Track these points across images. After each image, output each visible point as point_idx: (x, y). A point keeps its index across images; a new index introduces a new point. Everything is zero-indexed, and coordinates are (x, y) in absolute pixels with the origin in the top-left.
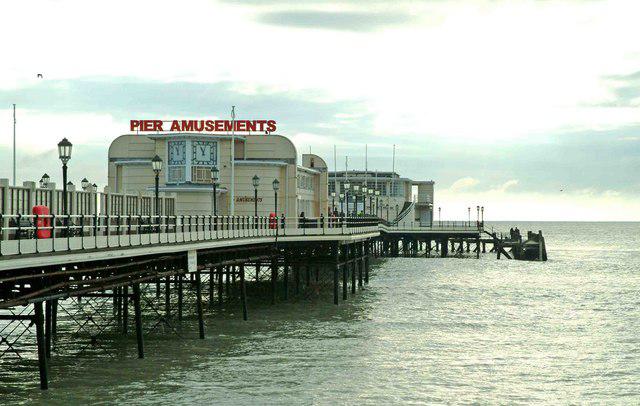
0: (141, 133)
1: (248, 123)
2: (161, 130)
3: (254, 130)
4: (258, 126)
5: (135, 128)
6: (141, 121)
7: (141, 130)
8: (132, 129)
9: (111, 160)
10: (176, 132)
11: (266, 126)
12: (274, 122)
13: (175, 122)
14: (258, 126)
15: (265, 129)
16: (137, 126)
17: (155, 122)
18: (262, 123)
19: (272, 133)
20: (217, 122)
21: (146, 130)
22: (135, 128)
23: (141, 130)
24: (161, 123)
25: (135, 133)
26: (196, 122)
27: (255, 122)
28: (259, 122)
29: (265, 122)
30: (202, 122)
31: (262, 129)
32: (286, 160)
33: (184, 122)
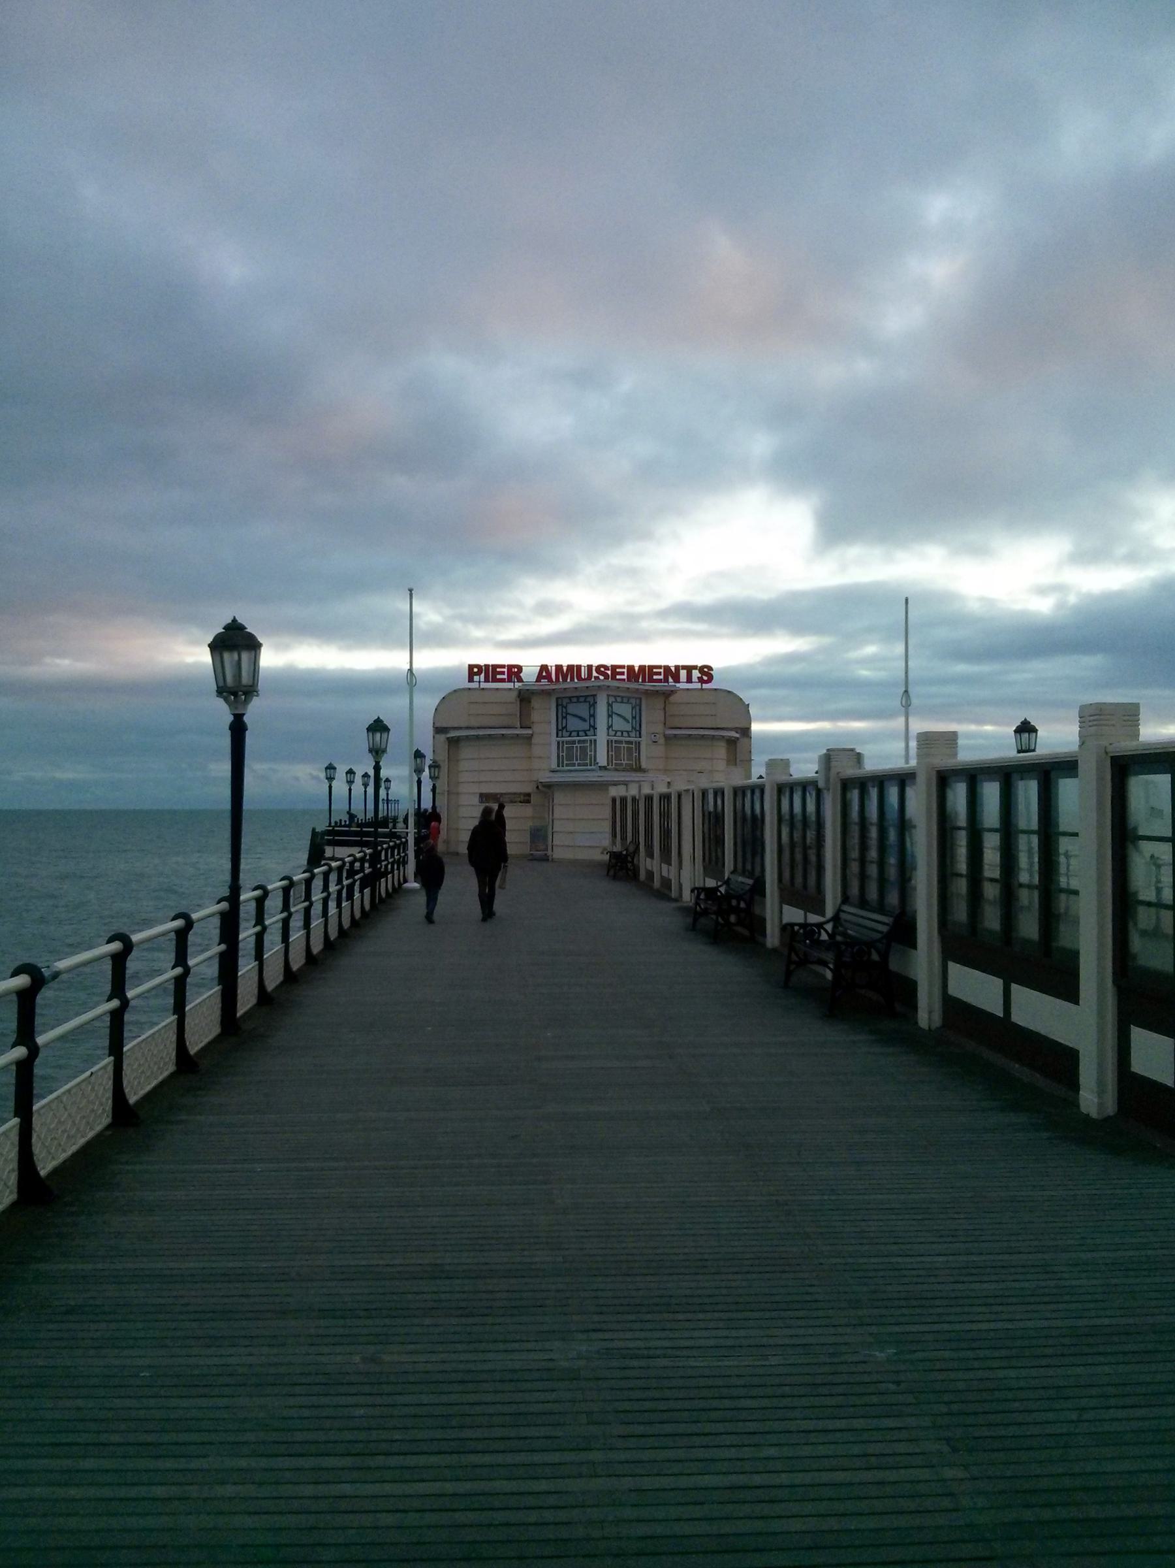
0: (483, 685)
1: (667, 668)
2: (520, 680)
3: (677, 679)
4: (683, 673)
5: (476, 678)
6: (487, 666)
7: (487, 680)
8: (471, 680)
9: (438, 730)
10: (544, 681)
11: (696, 674)
12: (710, 668)
13: (544, 668)
14: (683, 673)
15: (695, 679)
16: (479, 673)
17: (510, 667)
18: (689, 669)
19: (705, 686)
20: (614, 667)
21: (495, 680)
22: (476, 678)
23: (487, 680)
24: (520, 668)
25: (474, 685)
26: (579, 667)
27: (677, 667)
28: (684, 667)
29: (695, 667)
30: (590, 667)
31: (689, 680)
32: (736, 730)
33: (559, 668)
